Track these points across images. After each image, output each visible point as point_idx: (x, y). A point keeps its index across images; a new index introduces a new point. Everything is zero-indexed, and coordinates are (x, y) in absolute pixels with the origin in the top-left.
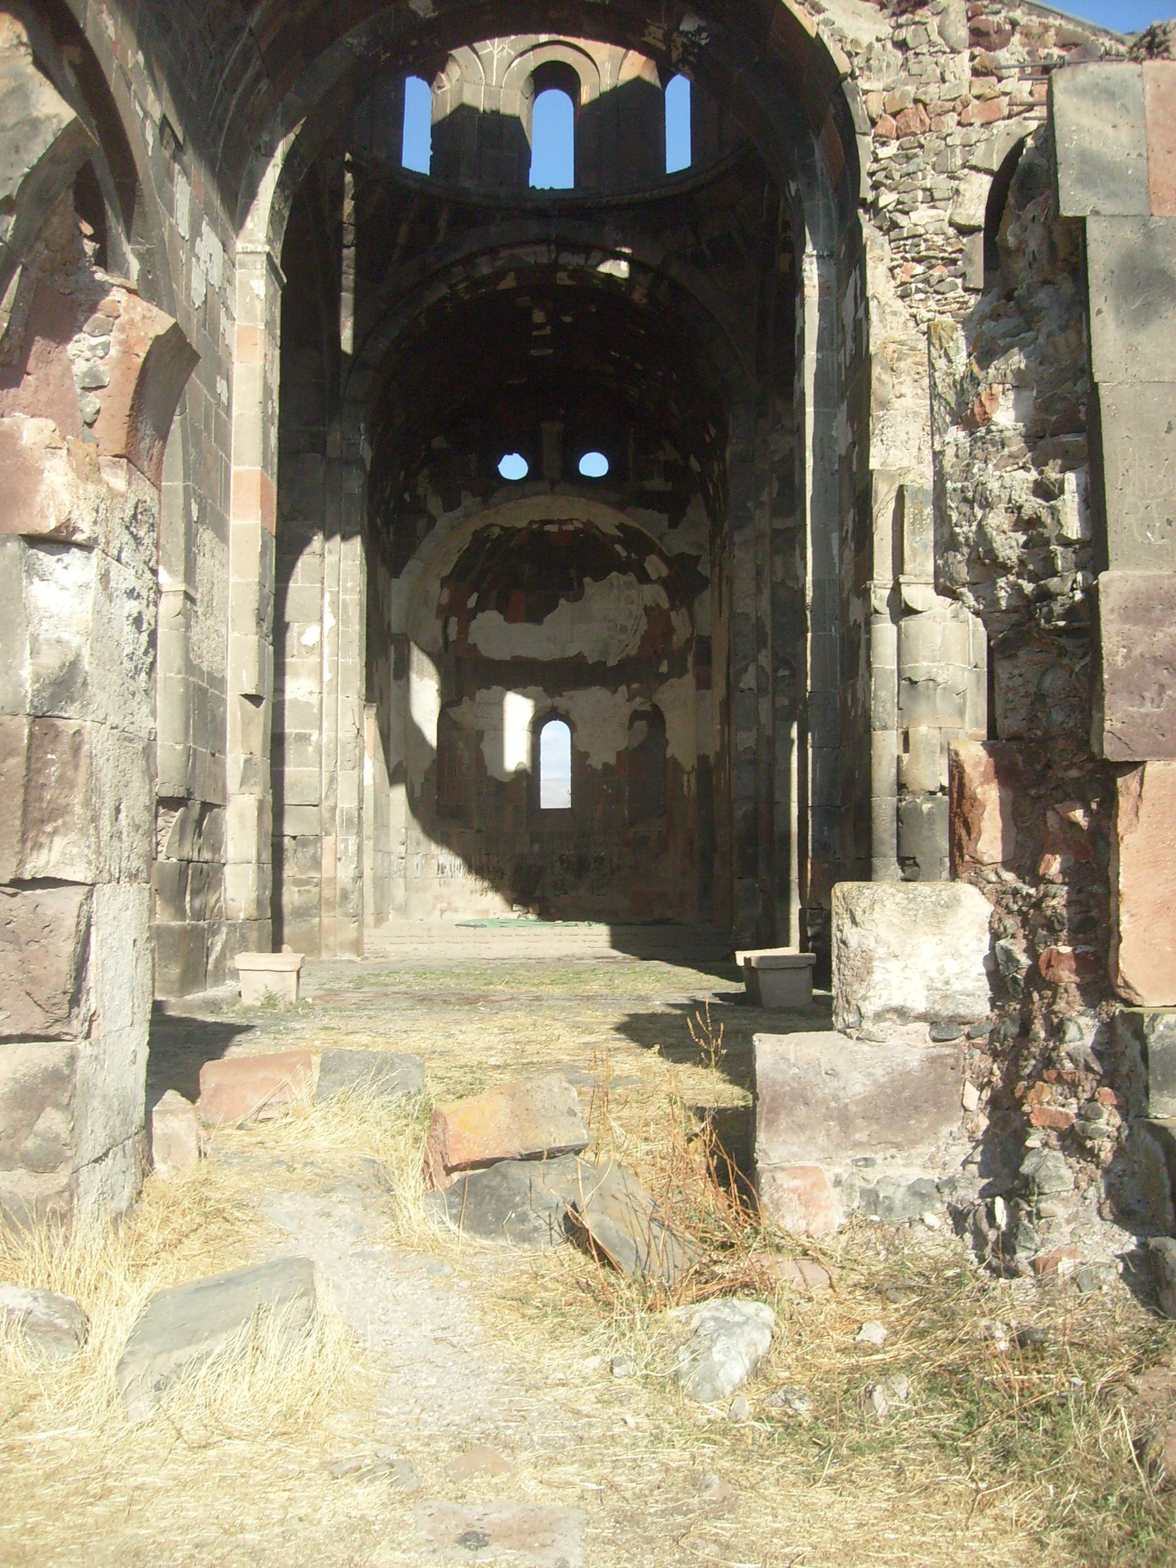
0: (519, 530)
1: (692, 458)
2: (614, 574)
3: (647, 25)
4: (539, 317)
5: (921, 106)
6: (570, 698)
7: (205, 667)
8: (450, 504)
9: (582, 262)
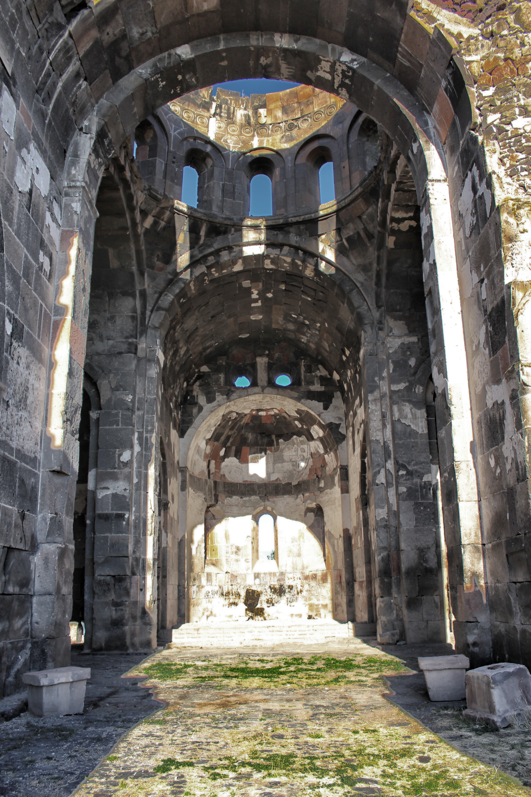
0: (246, 415)
1: (335, 373)
2: (295, 437)
3: (319, 61)
4: (255, 296)
5: (510, 62)
6: (274, 502)
7: (14, 445)
8: (210, 399)
9: (278, 253)
